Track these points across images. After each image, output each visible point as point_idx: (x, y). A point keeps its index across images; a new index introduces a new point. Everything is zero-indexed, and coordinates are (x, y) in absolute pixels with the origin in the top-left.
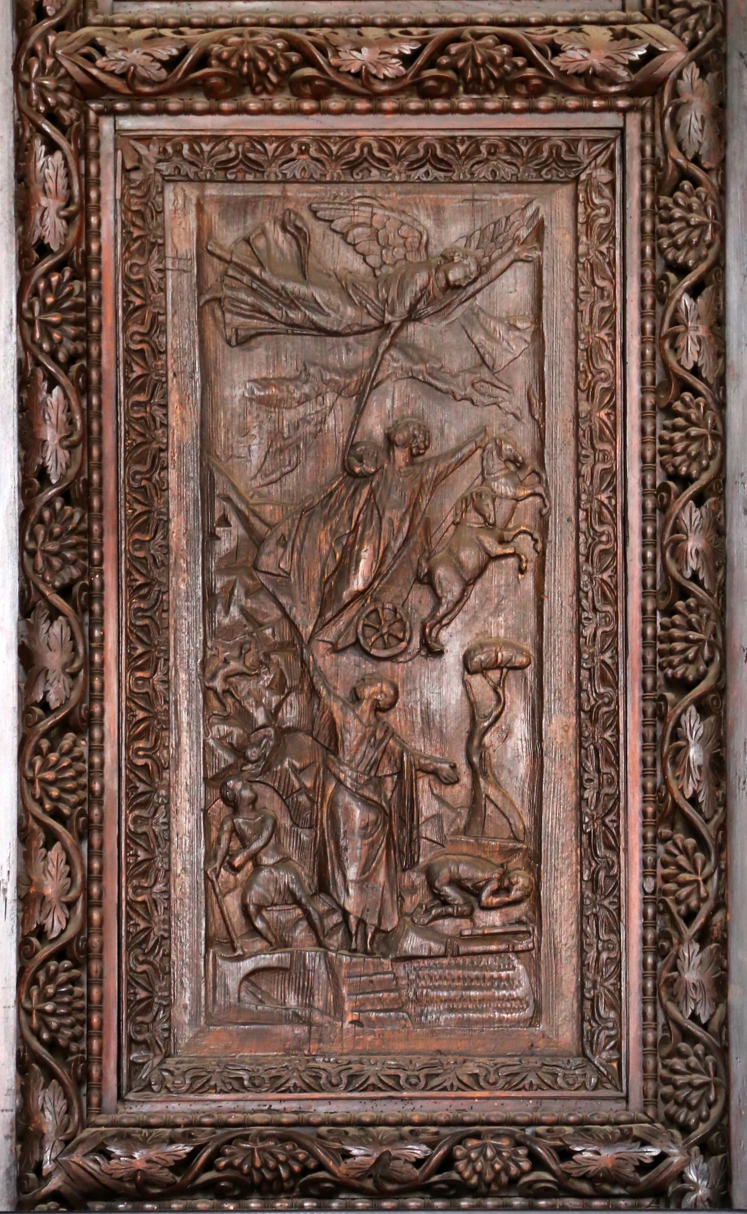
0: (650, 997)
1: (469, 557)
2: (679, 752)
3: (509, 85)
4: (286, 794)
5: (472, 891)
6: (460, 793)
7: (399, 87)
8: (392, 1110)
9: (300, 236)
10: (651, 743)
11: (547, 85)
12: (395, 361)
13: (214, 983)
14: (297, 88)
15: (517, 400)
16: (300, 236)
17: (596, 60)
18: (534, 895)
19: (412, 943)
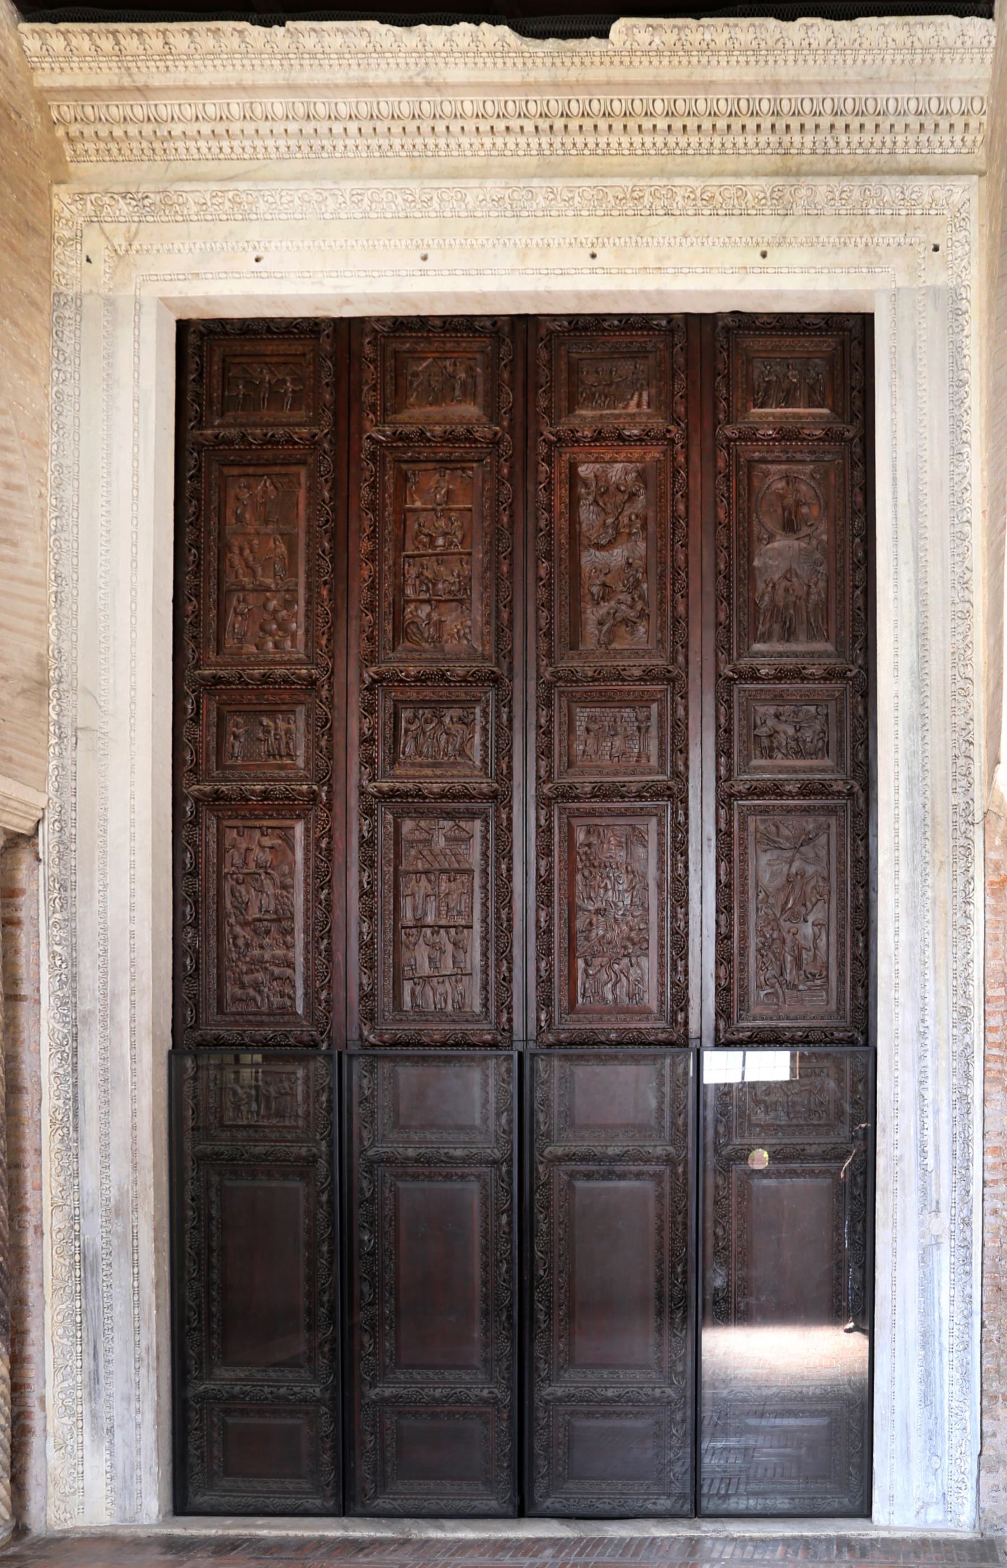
0: (852, 999)
1: (814, 900)
2: (857, 945)
3: (822, 793)
4: (774, 954)
5: (814, 975)
6: (811, 953)
7: (798, 794)
8: (796, 1025)
9: (777, 827)
10: (852, 942)
11: (830, 794)
12: (798, 856)
13: (758, 995)
14: (777, 794)
15: (824, 864)
16: (777, 827)
17: (840, 788)
18: (827, 976)
19: (801, 987)
